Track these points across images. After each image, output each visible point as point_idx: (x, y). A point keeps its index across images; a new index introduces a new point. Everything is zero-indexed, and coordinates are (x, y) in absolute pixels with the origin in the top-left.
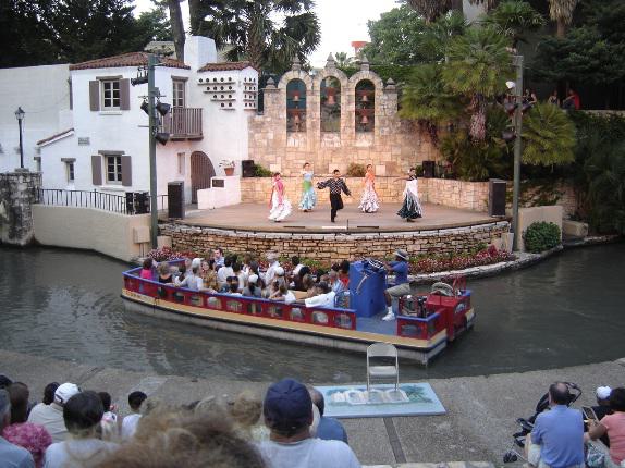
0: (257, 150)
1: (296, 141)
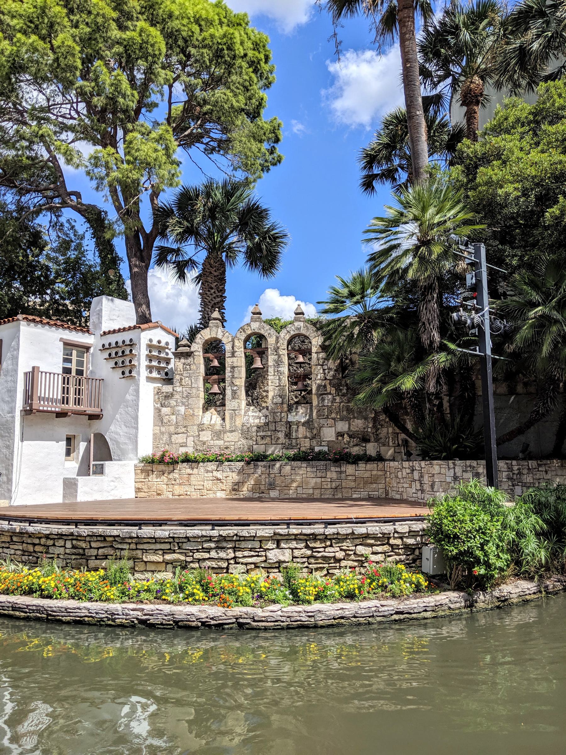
0: (163, 429)
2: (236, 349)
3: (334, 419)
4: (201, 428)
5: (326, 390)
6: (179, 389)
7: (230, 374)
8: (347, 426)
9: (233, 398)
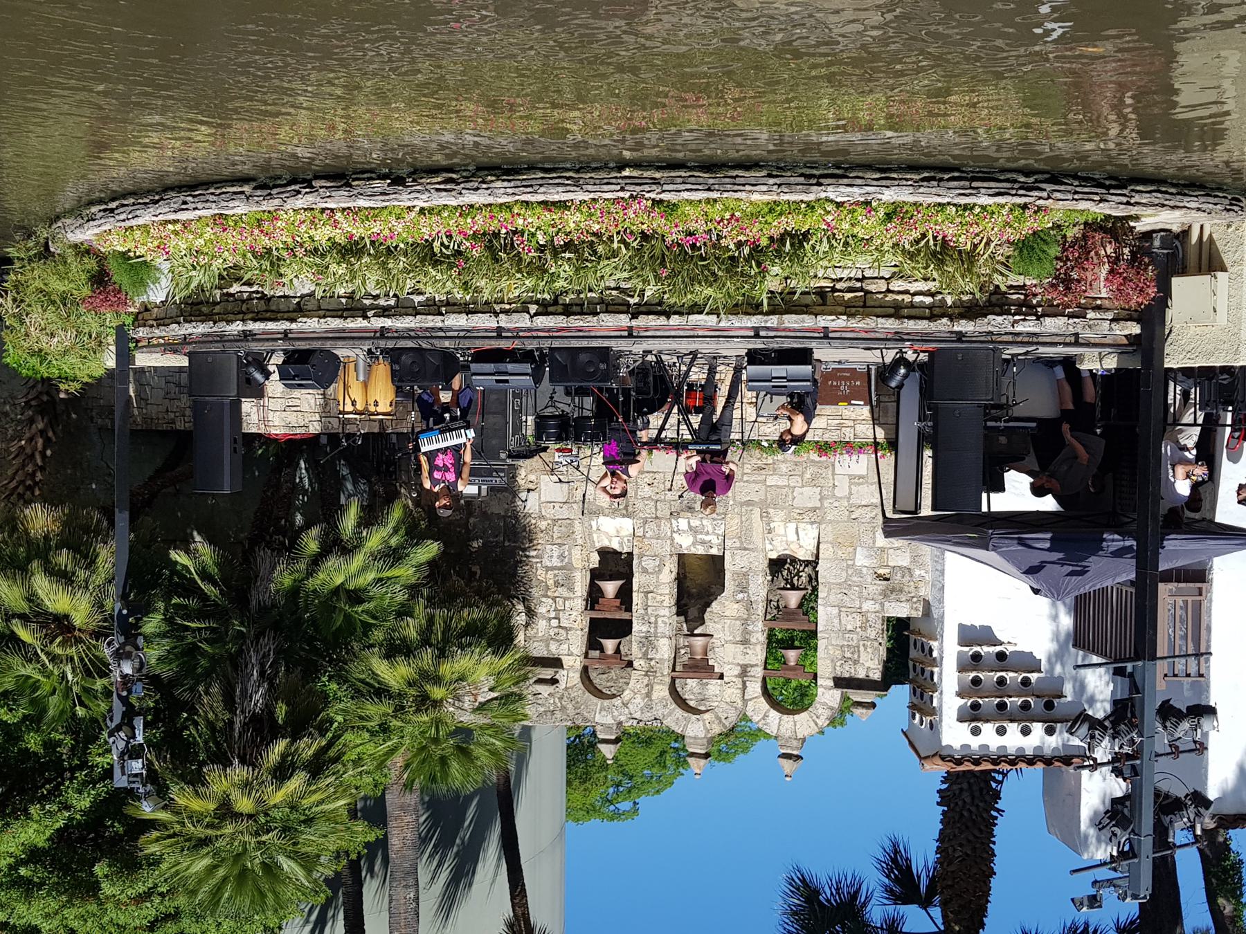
1: (797, 541)
2: (739, 681)
3: (542, 517)
4: (814, 515)
5: (555, 576)
6: (868, 606)
7: (750, 628)
9: (745, 575)
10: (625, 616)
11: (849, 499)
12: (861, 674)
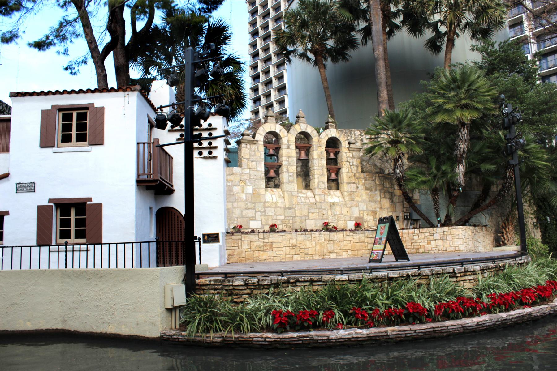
0: (235, 204)
1: (272, 196)
6: (247, 171)
8: (366, 206)
10: (329, 166)
11: (256, 212)
12: (248, 146)
